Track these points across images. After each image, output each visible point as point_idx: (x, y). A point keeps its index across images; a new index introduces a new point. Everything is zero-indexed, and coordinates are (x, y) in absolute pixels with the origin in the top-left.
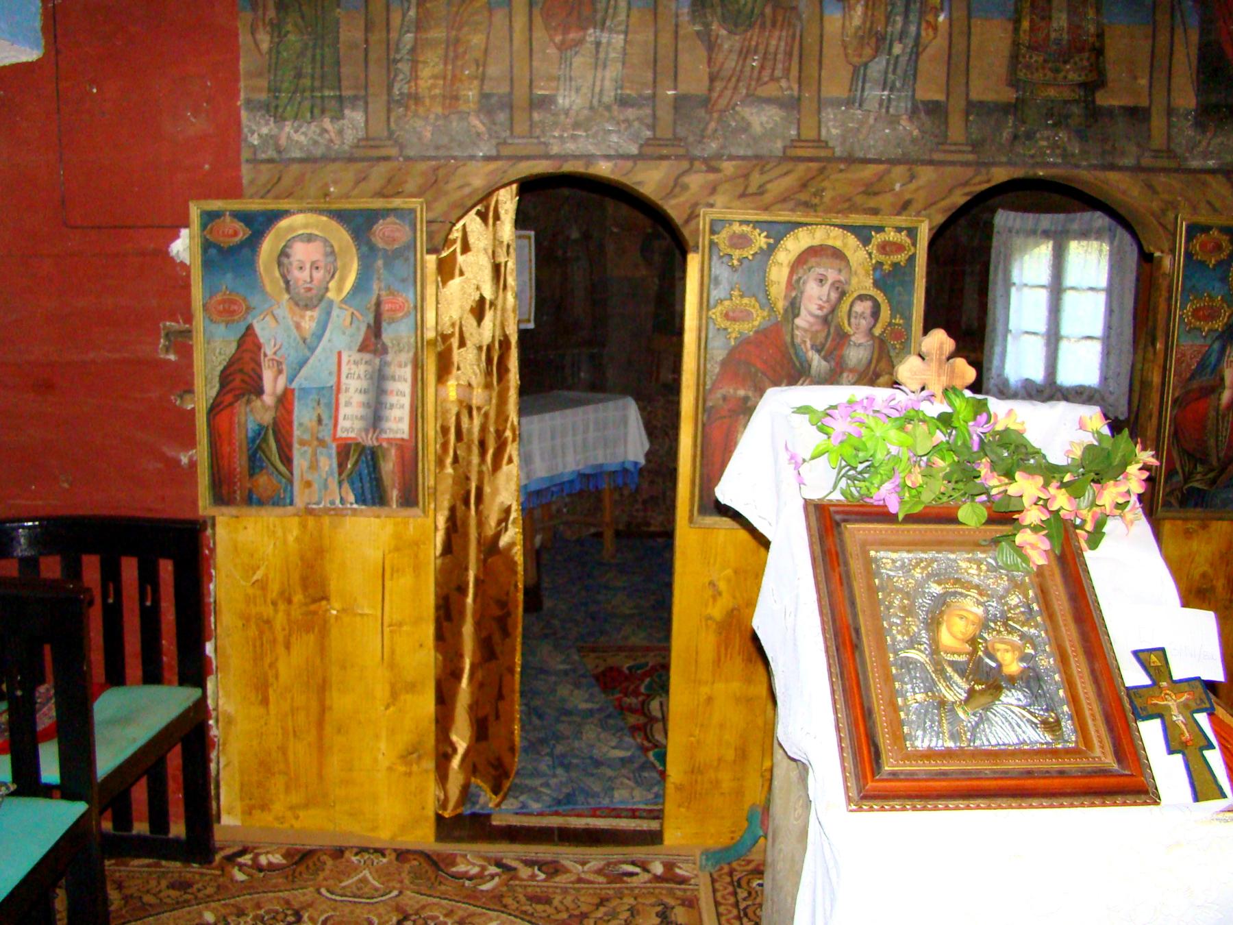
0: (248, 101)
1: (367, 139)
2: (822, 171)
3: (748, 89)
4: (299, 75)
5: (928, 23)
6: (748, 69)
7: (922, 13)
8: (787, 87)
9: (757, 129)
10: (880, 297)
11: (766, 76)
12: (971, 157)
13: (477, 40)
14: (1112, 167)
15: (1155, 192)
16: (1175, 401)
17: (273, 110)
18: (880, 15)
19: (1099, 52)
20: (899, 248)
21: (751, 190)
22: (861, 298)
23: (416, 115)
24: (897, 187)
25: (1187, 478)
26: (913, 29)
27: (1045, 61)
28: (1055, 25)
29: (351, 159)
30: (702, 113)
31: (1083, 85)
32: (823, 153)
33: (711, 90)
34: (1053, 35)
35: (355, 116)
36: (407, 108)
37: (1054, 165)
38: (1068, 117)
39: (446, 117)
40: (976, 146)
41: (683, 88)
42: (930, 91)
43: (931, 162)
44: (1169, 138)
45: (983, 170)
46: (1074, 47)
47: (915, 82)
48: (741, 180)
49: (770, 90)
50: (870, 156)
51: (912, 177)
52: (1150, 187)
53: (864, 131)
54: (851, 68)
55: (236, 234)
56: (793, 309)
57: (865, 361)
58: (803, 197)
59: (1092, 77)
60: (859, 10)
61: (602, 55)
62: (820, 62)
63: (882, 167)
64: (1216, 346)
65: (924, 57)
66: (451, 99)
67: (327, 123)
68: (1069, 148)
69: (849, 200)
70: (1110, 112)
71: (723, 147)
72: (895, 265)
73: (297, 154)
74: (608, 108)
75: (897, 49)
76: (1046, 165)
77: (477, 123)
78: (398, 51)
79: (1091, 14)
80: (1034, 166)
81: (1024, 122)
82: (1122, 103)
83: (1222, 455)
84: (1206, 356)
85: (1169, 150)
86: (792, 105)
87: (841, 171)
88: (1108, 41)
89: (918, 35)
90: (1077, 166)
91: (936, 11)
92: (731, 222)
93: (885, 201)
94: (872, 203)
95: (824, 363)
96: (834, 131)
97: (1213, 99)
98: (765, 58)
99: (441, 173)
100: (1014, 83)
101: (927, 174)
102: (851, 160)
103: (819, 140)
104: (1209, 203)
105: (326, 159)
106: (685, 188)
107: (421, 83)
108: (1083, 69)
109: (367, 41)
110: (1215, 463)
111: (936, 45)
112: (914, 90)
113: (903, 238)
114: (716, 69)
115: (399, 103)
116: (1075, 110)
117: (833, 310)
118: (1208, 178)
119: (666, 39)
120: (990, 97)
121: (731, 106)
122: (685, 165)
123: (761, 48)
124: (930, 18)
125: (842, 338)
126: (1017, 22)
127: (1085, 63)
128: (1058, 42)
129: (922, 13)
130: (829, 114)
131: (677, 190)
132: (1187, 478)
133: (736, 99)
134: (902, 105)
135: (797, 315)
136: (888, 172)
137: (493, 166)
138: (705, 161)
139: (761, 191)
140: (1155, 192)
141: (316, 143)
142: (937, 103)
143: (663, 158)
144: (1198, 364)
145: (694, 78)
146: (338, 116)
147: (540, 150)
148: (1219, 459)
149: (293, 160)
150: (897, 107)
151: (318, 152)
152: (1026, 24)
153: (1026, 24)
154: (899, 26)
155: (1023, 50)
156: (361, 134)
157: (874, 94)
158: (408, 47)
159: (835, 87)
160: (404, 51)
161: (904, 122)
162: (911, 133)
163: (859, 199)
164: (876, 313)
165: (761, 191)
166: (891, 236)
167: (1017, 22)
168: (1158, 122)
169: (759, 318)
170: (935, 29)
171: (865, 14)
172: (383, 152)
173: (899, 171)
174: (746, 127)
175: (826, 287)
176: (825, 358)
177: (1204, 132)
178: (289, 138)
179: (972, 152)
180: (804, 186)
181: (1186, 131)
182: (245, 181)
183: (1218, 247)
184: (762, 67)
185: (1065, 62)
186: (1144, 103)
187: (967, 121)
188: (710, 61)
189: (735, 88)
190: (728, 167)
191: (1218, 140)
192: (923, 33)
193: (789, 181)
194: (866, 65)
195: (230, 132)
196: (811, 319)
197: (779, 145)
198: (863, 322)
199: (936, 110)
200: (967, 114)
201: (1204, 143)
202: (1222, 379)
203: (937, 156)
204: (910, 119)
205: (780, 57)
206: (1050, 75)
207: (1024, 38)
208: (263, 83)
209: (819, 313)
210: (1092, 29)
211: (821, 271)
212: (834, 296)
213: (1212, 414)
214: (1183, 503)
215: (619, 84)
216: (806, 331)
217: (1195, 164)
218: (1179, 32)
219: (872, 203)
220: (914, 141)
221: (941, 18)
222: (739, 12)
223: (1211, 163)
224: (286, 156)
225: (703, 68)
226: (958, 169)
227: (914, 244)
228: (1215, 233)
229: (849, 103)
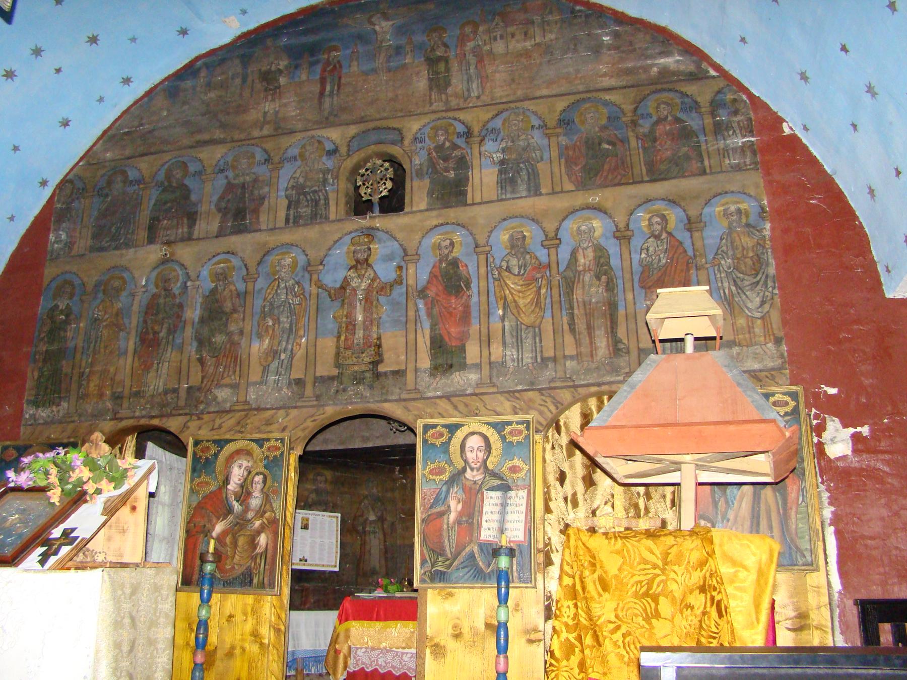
0: (27, 400)
1: (68, 413)
2: (246, 416)
3: (218, 381)
4: (46, 388)
5: (297, 343)
6: (218, 373)
7: (295, 339)
8: (234, 379)
9: (220, 399)
10: (267, 472)
11: (225, 375)
12: (315, 403)
13: (112, 369)
14: (386, 401)
15: (409, 411)
16: (423, 521)
17: (36, 404)
18: (276, 342)
19: (379, 346)
20: (277, 448)
21: (215, 427)
22: (257, 474)
23: (87, 402)
24: (280, 420)
25: (433, 566)
26: (290, 346)
27: (353, 354)
28: (357, 336)
29: (60, 422)
30: (198, 394)
31: (372, 363)
32: (246, 407)
33: (202, 382)
34: (355, 342)
35: (65, 404)
36: (84, 399)
37: (356, 403)
38: (364, 379)
39: (97, 403)
40: (318, 397)
41: (190, 384)
42: (297, 374)
43: (296, 407)
44: (416, 384)
45: (322, 409)
46: (367, 344)
47: (291, 370)
48: (211, 423)
49: (227, 381)
50: (268, 407)
51: (287, 415)
52: (406, 408)
53: (266, 395)
54: (262, 368)
55: (13, 455)
56: (227, 481)
57: (259, 506)
58: (238, 428)
59: (377, 358)
60: (267, 341)
61: (159, 372)
62: (249, 366)
63: (274, 411)
64: (444, 488)
65: (295, 359)
66: (101, 395)
67: (54, 408)
68: (364, 394)
69: (259, 428)
70: (385, 373)
71: (205, 408)
72: (275, 457)
73: (41, 421)
74: (160, 394)
75: (283, 356)
76: (351, 403)
77: (109, 405)
78: (82, 376)
79: (375, 329)
80: (347, 404)
81: (341, 383)
82: (392, 369)
83: (453, 550)
84: (438, 494)
85: (416, 389)
86: (235, 387)
87: (255, 415)
88: (383, 341)
89: (292, 349)
90: (369, 402)
91: (301, 337)
92: (202, 441)
93: (275, 426)
94: (268, 429)
95: (240, 507)
96: (253, 397)
97: (440, 361)
98: (225, 367)
99: (93, 427)
100: (338, 365)
101: (294, 413)
102: (259, 409)
103: (246, 401)
104: (440, 414)
105: (52, 422)
106: (188, 428)
107: (90, 389)
108: (371, 355)
109: (72, 373)
110: (449, 556)
111: (300, 353)
112: (290, 374)
113: (279, 444)
114: (204, 374)
115: (81, 398)
116: (368, 375)
117: (246, 480)
118: (438, 401)
119: (185, 362)
120: (325, 374)
121: (209, 390)
122: (188, 417)
123: (224, 364)
124: (298, 341)
125: (249, 494)
126: (339, 337)
127: (373, 352)
128: (358, 344)
129: (295, 339)
130: (251, 389)
131: (185, 429)
132: (433, 566)
133: (214, 384)
134: (284, 382)
135: (228, 484)
136: (276, 414)
137: (112, 423)
138: (197, 415)
139: (220, 427)
140: (409, 411)
141: (49, 416)
142: (299, 379)
143: (180, 415)
144: (435, 499)
145: (195, 378)
146: (58, 405)
147: (132, 415)
148: (451, 552)
149: (40, 424)
150: (282, 383)
151: (49, 420)
152: (343, 338)
153: (343, 338)
154: (284, 346)
155: (342, 350)
156: (66, 412)
157: (272, 378)
158: (87, 374)
159: (255, 377)
160: (85, 376)
161: (285, 390)
162: (287, 394)
163: (263, 428)
164: (265, 481)
165: (220, 427)
166: (272, 443)
167: (339, 337)
168: (410, 376)
169: (213, 488)
170: (300, 345)
171: (269, 342)
172: (72, 419)
173: (282, 412)
174: (215, 398)
175: (243, 469)
176: (240, 505)
177: (435, 379)
178: (40, 415)
179: (317, 400)
180: (239, 423)
181: (425, 378)
182: (21, 434)
183: (442, 435)
184: (224, 372)
185: (363, 353)
186: (403, 368)
187: (314, 385)
188: (202, 371)
189: (213, 381)
190: (206, 417)
191: (443, 381)
192: (294, 348)
193: (232, 422)
194: (269, 366)
195: (18, 415)
196: (235, 485)
197: (228, 405)
198: (259, 486)
199: (300, 382)
200: (315, 383)
201: (435, 384)
202: (449, 507)
203: (299, 404)
204: (288, 388)
205: (232, 365)
206: (355, 360)
207: (342, 344)
208: (33, 392)
209: (239, 482)
210: (375, 336)
211: (240, 462)
212: (246, 473)
213: (445, 527)
214: (432, 580)
215: (165, 385)
216: (233, 491)
217: (429, 395)
218: (419, 331)
219: (268, 429)
220: (289, 398)
221: (303, 340)
222: (216, 348)
223: (439, 393)
224: (38, 422)
225: (200, 374)
226: (310, 409)
227: (284, 446)
228: (439, 428)
229: (261, 383)
